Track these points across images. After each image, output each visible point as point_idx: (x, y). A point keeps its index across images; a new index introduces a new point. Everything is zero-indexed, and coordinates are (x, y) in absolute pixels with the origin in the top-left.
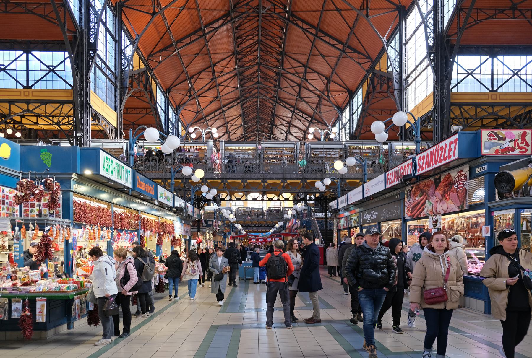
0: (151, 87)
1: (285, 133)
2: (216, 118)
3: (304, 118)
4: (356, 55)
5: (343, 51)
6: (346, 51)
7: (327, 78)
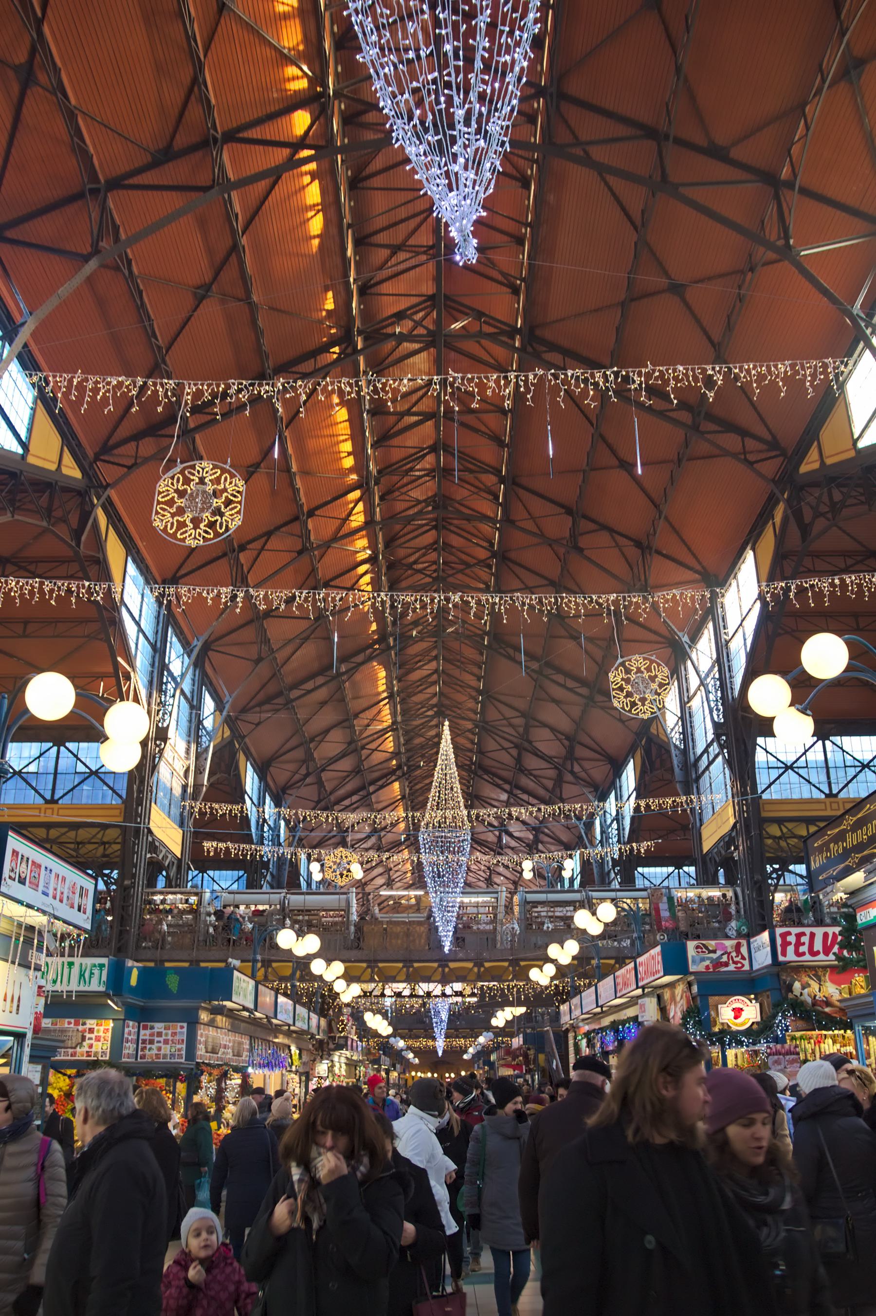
1: (516, 746)
3: (570, 690)
4: (731, 441)
5: (695, 427)
6: (702, 428)
7: (638, 544)
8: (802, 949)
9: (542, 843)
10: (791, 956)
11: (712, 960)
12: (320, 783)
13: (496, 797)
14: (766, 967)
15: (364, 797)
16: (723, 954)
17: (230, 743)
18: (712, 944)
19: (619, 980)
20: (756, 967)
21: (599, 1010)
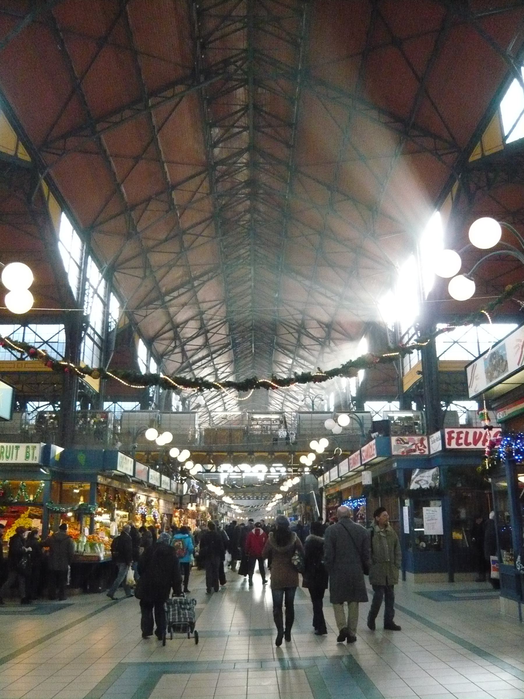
0: (44, 203)
1: (298, 332)
2: (183, 299)
8: (461, 441)
9: (312, 388)
10: (454, 445)
11: (406, 447)
12: (183, 352)
13: (285, 362)
14: (438, 452)
15: (210, 361)
16: (413, 445)
17: (130, 327)
18: (406, 438)
19: (351, 461)
20: (432, 452)
21: (340, 479)
